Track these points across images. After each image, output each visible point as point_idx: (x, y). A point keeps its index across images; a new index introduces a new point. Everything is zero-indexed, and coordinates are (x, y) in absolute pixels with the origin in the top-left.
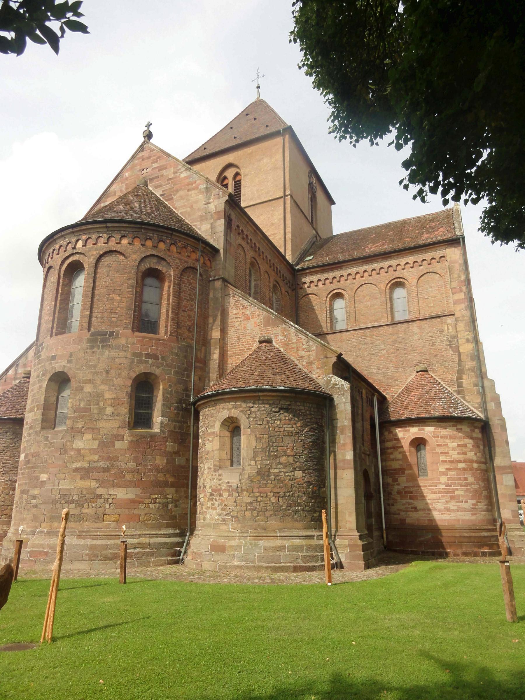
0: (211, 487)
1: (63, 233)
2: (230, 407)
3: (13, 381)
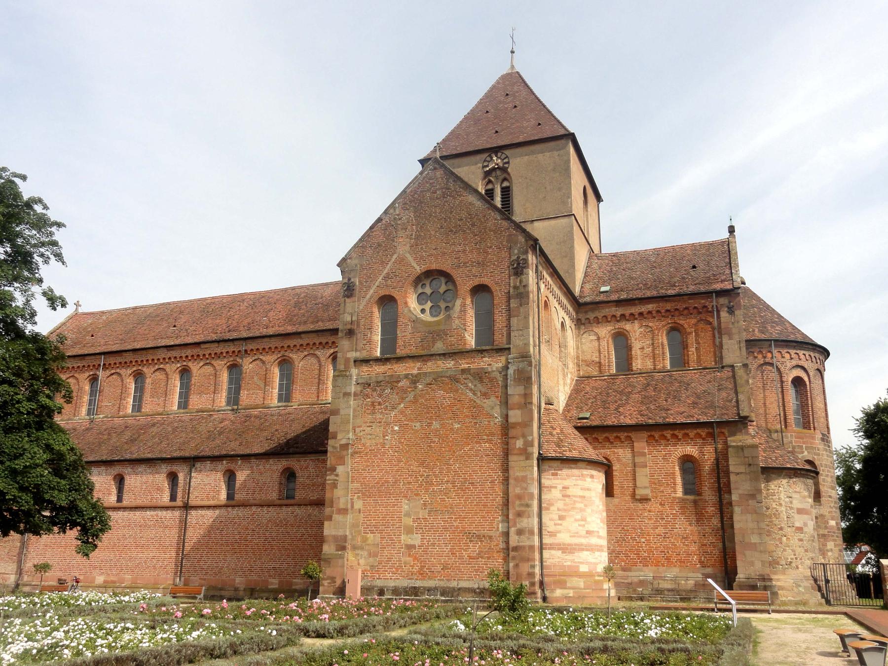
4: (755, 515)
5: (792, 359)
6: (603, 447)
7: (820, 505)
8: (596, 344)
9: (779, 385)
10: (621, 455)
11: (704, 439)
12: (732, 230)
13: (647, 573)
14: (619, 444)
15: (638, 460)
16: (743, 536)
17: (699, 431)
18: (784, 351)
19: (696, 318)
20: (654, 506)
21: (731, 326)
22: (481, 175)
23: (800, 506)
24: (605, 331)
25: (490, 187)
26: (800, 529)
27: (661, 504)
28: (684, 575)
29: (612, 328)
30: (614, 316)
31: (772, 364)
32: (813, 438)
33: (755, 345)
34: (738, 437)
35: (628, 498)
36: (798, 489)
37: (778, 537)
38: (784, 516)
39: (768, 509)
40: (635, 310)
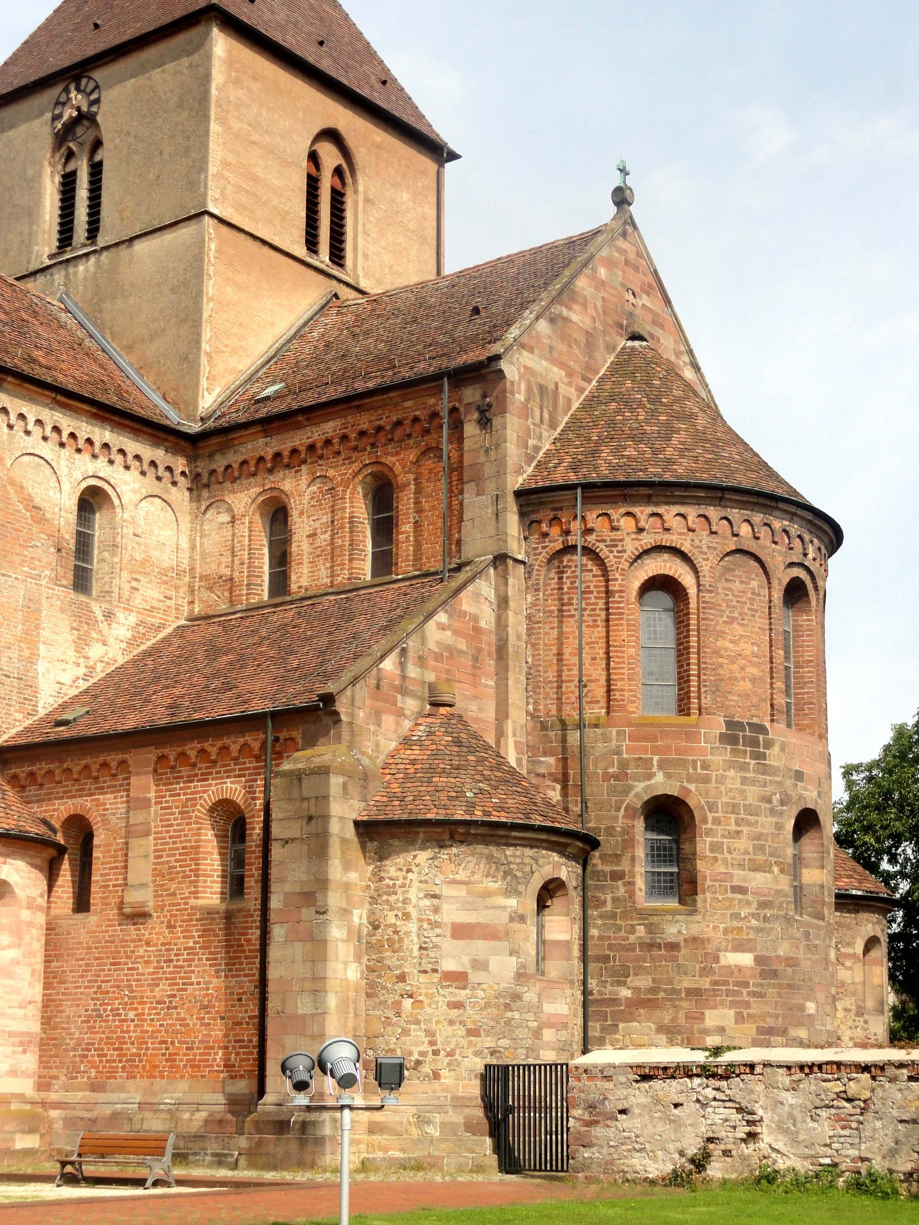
0: (851, 1039)
1: (799, 512)
3: (399, 697)
4: (309, 945)
5: (641, 530)
6: (81, 793)
7: (693, 912)
8: (227, 532)
10: (106, 809)
11: (257, 758)
12: (621, 198)
13: (126, 1096)
14: (89, 784)
15: (137, 817)
16: (284, 1001)
17: (248, 738)
18: (616, 513)
19: (417, 444)
20: (155, 930)
21: (482, 459)
22: (47, 140)
23: (463, 917)
24: (244, 499)
25: (70, 168)
26: (458, 979)
27: (170, 926)
28: (196, 1098)
29: (259, 490)
30: (261, 459)
32: (691, 735)
33: (541, 504)
35: (113, 913)
36: (462, 875)
38: (412, 944)
39: (376, 927)
40: (300, 439)
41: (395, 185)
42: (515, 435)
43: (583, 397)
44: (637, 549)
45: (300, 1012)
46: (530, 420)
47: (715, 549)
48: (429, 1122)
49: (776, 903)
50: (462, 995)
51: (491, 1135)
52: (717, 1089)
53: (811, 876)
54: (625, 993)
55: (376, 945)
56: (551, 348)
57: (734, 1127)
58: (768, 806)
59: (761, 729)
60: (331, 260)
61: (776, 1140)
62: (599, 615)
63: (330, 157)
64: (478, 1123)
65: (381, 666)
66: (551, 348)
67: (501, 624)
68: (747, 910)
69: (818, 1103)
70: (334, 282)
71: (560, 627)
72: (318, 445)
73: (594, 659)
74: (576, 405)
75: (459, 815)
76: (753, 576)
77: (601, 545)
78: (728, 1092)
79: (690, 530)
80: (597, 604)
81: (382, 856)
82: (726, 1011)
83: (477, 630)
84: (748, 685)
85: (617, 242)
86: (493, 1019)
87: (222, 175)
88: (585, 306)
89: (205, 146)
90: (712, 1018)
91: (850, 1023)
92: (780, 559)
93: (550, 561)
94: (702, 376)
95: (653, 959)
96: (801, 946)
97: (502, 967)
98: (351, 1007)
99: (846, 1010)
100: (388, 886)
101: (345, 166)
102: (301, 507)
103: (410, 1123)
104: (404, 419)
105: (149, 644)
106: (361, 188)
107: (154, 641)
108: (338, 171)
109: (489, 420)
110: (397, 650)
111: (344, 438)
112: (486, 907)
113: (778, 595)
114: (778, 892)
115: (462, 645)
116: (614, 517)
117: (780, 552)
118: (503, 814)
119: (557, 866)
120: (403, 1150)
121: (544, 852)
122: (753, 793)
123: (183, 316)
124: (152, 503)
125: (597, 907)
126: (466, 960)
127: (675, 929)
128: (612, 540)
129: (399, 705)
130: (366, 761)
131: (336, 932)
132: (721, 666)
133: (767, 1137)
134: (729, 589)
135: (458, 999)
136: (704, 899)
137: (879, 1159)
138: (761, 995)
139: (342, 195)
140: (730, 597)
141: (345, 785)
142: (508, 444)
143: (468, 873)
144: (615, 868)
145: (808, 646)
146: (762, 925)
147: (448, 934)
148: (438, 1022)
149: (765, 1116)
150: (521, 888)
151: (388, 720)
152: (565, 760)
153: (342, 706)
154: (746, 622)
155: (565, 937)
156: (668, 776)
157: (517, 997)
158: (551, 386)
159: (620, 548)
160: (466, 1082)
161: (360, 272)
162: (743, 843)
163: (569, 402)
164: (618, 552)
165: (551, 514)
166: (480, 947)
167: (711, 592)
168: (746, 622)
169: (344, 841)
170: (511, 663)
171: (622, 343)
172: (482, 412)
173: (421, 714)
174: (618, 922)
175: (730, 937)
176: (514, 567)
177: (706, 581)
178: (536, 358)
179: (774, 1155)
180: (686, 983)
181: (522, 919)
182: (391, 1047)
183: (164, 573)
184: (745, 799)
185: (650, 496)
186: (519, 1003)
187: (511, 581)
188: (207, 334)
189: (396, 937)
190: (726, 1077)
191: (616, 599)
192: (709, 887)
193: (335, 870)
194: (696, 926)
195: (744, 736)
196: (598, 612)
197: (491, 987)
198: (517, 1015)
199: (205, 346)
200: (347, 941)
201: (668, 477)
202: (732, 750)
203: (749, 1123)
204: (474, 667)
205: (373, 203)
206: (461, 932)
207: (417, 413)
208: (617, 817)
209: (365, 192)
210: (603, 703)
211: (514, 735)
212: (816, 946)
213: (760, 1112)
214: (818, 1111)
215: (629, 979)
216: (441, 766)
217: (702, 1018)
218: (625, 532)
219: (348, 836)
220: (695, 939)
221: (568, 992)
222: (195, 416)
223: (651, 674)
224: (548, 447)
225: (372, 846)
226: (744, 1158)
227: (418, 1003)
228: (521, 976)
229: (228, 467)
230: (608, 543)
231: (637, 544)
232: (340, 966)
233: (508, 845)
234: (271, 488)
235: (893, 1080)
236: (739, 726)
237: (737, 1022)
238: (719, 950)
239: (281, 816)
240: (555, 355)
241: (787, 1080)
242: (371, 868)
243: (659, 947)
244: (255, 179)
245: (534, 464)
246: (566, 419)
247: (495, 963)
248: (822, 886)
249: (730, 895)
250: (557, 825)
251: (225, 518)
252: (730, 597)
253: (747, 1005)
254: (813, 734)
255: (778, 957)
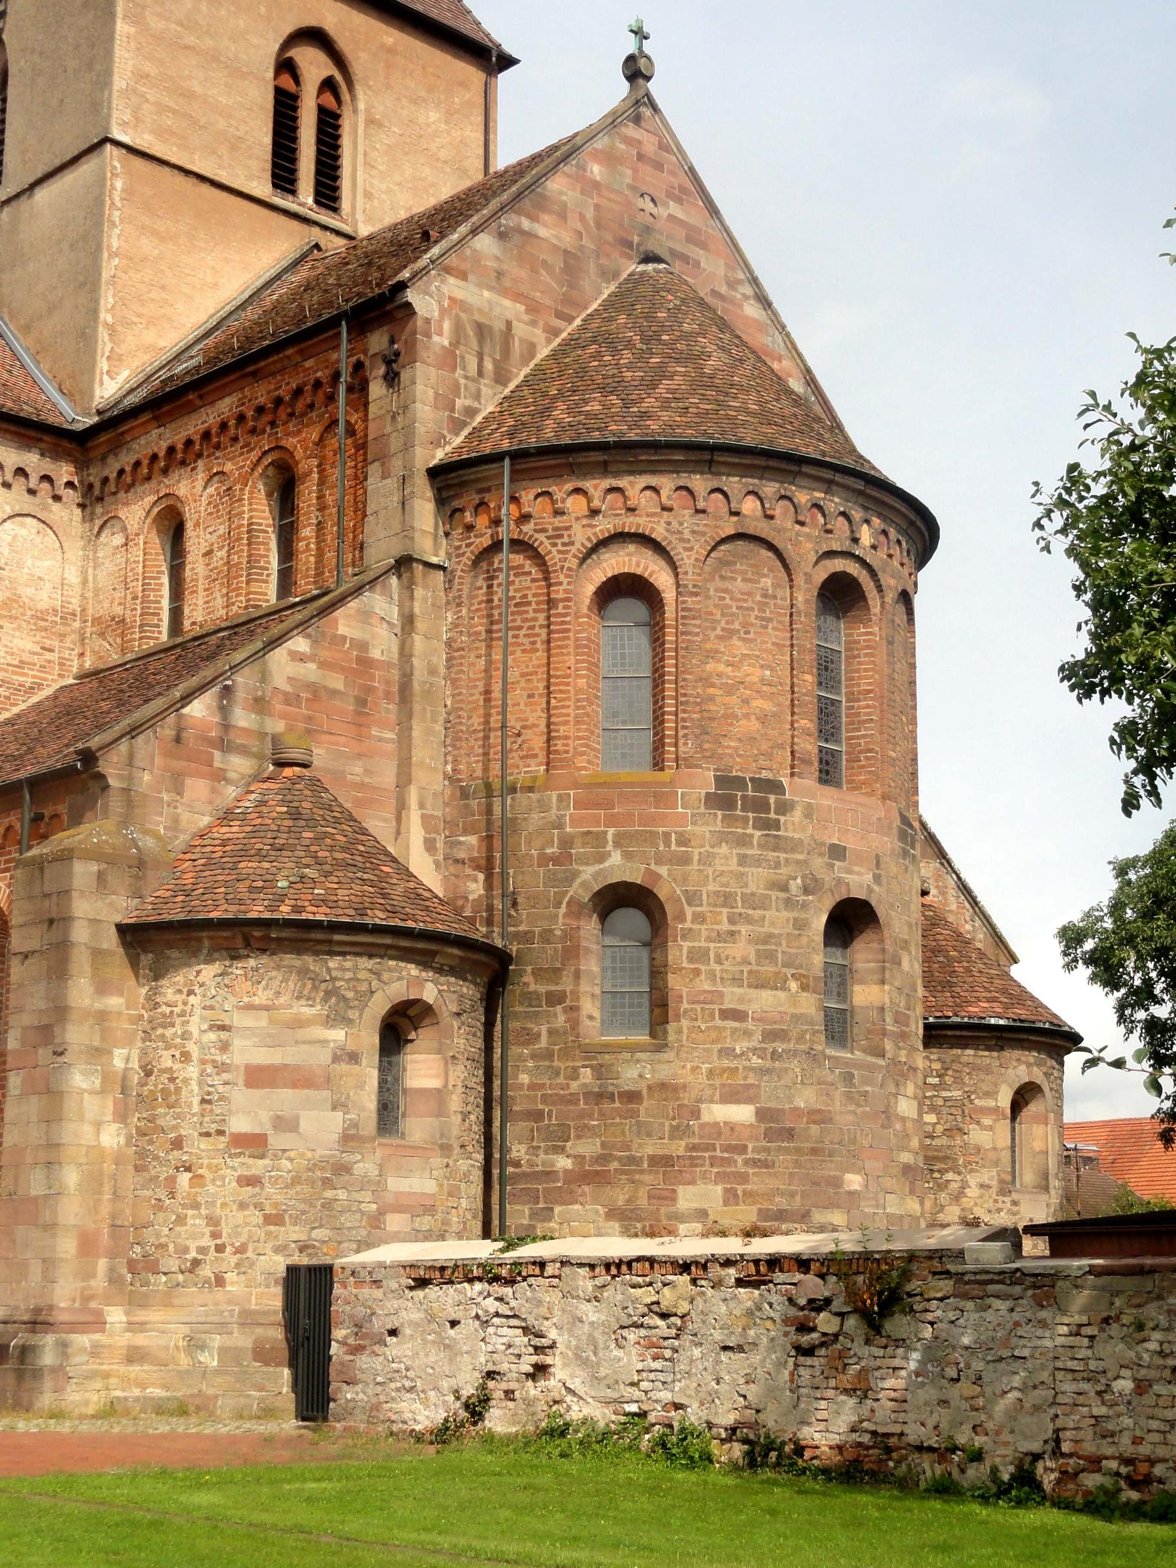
1: (838, 478)
2: (1032, 1060)
3: (217, 754)
7: (660, 1048)
9: (541, 617)
12: (636, 71)
16: (16, 1178)
18: (560, 490)
21: (388, 429)
23: (261, 1057)
24: (136, 511)
26: (253, 1143)
31: (496, 546)
32: (663, 798)
33: (463, 484)
34: (84, 828)
36: (262, 997)
37: (165, 1173)
38: (192, 1095)
39: (148, 1074)
40: (193, 426)
41: (416, 101)
42: (431, 392)
43: (558, 340)
44: (589, 539)
45: (33, 1193)
46: (459, 371)
47: (703, 534)
48: (202, 1347)
49: (794, 1034)
50: (258, 1166)
51: (291, 1366)
52: (500, 1299)
53: (865, 995)
54: (563, 1163)
55: (144, 1100)
56: (500, 274)
57: (519, 1356)
58: (782, 895)
59: (775, 787)
60: (317, 202)
61: (572, 1376)
62: (538, 635)
63: (314, 66)
64: (272, 1348)
65: (185, 711)
66: (500, 274)
67: (405, 654)
68: (745, 1044)
69: (626, 1321)
70: (316, 230)
71: (489, 655)
72: (213, 431)
73: (530, 696)
74: (543, 352)
75: (257, 911)
76: (766, 571)
77: (541, 537)
78: (513, 1303)
79: (664, 509)
80: (535, 619)
81: (158, 975)
82: (710, 1187)
83: (365, 663)
84: (754, 725)
85: (623, 130)
86: (304, 1201)
87: (134, 90)
88: (563, 216)
89: (109, 53)
90: (687, 1198)
91: (990, 1205)
92: (809, 546)
93: (476, 562)
94: (775, 314)
95: (602, 1115)
96: (838, 1095)
97: (320, 1127)
98: (107, 1187)
99: (982, 1186)
100: (164, 1015)
101: (339, 77)
102: (195, 517)
103: (177, 1347)
104: (305, 384)
105: (15, 710)
106: (361, 106)
107: (23, 706)
108: (328, 85)
109: (397, 374)
110: (216, 689)
111: (241, 418)
112: (297, 1042)
113: (805, 596)
114: (796, 1018)
115: (337, 682)
116: (558, 496)
117: (808, 535)
118: (324, 909)
119: (420, 983)
120: (166, 1387)
121: (392, 963)
122: (757, 878)
123: (81, 278)
124: (22, 525)
125: (526, 1043)
126: (265, 1116)
127: (633, 1073)
128: (555, 529)
129: (217, 764)
130: (148, 842)
131: (80, 1079)
132: (712, 699)
133: (560, 1372)
134: (726, 591)
135: (253, 1172)
136: (679, 1029)
137: (695, 1405)
138: (766, 1164)
139: (337, 117)
140: (728, 601)
141: (100, 875)
142: (418, 405)
143: (270, 993)
144: (553, 988)
145: (866, 670)
146: (768, 1064)
147: (241, 1081)
148: (224, 1205)
149: (559, 1340)
150: (353, 1014)
151: (197, 788)
152: (489, 838)
153: (111, 767)
154: (751, 636)
155: (434, 1083)
156: (628, 856)
157: (343, 1169)
158: (499, 326)
159: (566, 540)
160: (262, 1289)
161: (360, 217)
162: (741, 949)
163: (531, 349)
164: (564, 544)
165: (476, 499)
166: (285, 1098)
167: (696, 594)
168: (751, 636)
169: (97, 954)
170: (417, 707)
171: (633, 267)
172: (389, 363)
173: (259, 778)
174: (556, 1063)
175: (717, 1082)
176: (424, 576)
177: (690, 577)
178: (473, 288)
179: (569, 1398)
180: (650, 1148)
181: (354, 1058)
182: (163, 1240)
183: (40, 616)
184: (746, 885)
185: (605, 463)
186: (346, 1178)
187: (419, 592)
188: (108, 299)
189: (172, 1087)
190: (511, 1282)
191: (560, 610)
192: (686, 1011)
193: (81, 992)
194: (666, 1067)
195: (744, 797)
196: (537, 630)
197: (302, 1155)
198: (342, 1194)
199: (105, 316)
200: (102, 1092)
201: (633, 436)
202: (724, 817)
203: (538, 1350)
204: (359, 713)
205: (381, 125)
206: (258, 1077)
207: (319, 374)
208: (557, 916)
209: (367, 110)
210: (542, 758)
211: (422, 806)
212: (865, 1094)
213: (553, 1334)
214: (625, 1332)
215: (569, 1144)
216: (258, 846)
217: (672, 1198)
218: (572, 515)
219: (105, 946)
220: (663, 1086)
221: (437, 1161)
222: (90, 408)
223: (615, 715)
224: (491, 409)
225: (146, 959)
226: (529, 1403)
227: (198, 1180)
228: (349, 1139)
229: (121, 472)
230: (551, 533)
231: (589, 532)
232: (87, 1129)
233: (332, 953)
234: (167, 495)
235: (717, 1285)
236: (740, 782)
237: (726, 1203)
238: (700, 1100)
239: (21, 920)
240: (507, 283)
241: (589, 1285)
242: (144, 990)
243: (611, 1097)
244: (189, 95)
245: (465, 432)
246: (526, 370)
247: (307, 1122)
248: (882, 1009)
249: (718, 1022)
250: (410, 924)
251: (118, 540)
252: (728, 601)
253: (744, 1178)
254: (872, 793)
255: (796, 1109)
